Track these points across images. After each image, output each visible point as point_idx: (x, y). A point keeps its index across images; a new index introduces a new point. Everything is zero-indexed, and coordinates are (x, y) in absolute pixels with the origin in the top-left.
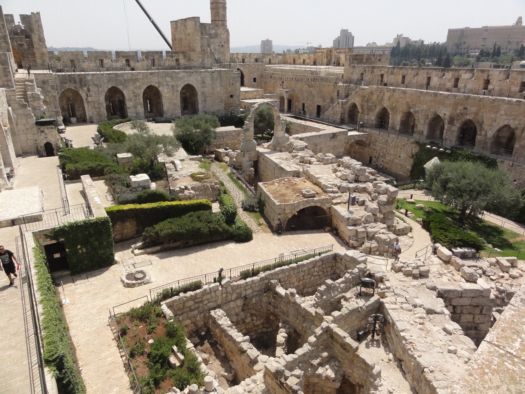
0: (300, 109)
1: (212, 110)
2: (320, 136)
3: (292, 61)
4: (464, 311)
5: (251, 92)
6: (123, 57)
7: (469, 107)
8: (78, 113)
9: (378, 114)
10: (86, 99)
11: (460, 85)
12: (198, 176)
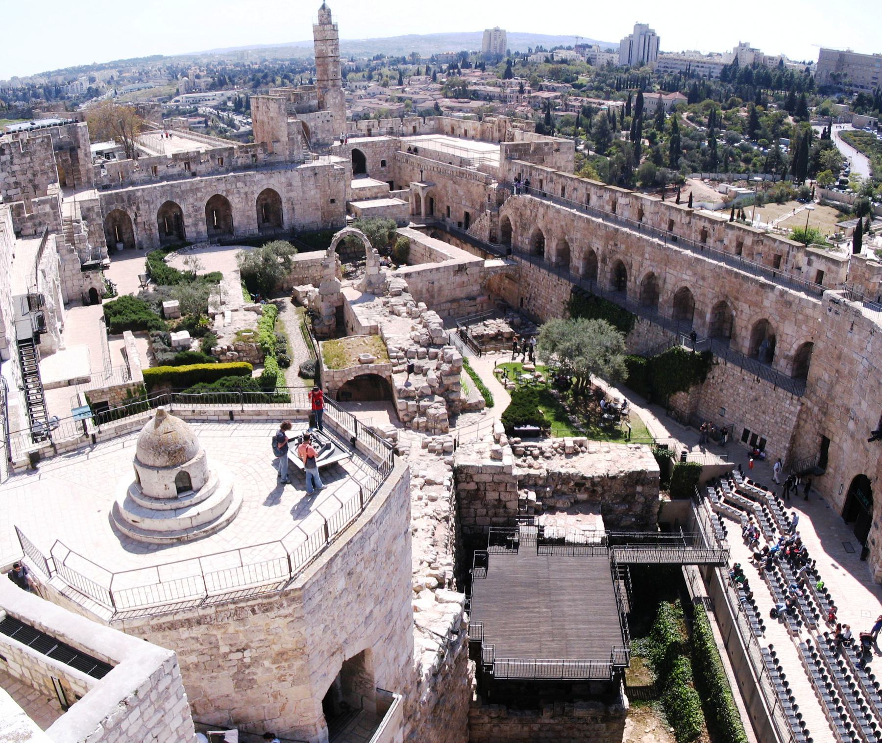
0: (443, 214)
1: (302, 221)
2: (438, 269)
3: (450, 129)
4: (488, 488)
5: (370, 188)
6: (182, 160)
7: (619, 243)
8: (125, 237)
9: (533, 236)
10: (135, 220)
11: (618, 211)
12: (244, 334)
